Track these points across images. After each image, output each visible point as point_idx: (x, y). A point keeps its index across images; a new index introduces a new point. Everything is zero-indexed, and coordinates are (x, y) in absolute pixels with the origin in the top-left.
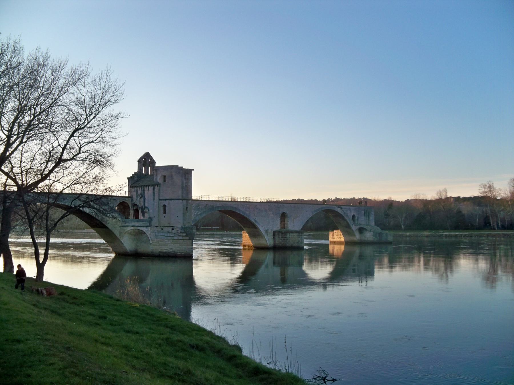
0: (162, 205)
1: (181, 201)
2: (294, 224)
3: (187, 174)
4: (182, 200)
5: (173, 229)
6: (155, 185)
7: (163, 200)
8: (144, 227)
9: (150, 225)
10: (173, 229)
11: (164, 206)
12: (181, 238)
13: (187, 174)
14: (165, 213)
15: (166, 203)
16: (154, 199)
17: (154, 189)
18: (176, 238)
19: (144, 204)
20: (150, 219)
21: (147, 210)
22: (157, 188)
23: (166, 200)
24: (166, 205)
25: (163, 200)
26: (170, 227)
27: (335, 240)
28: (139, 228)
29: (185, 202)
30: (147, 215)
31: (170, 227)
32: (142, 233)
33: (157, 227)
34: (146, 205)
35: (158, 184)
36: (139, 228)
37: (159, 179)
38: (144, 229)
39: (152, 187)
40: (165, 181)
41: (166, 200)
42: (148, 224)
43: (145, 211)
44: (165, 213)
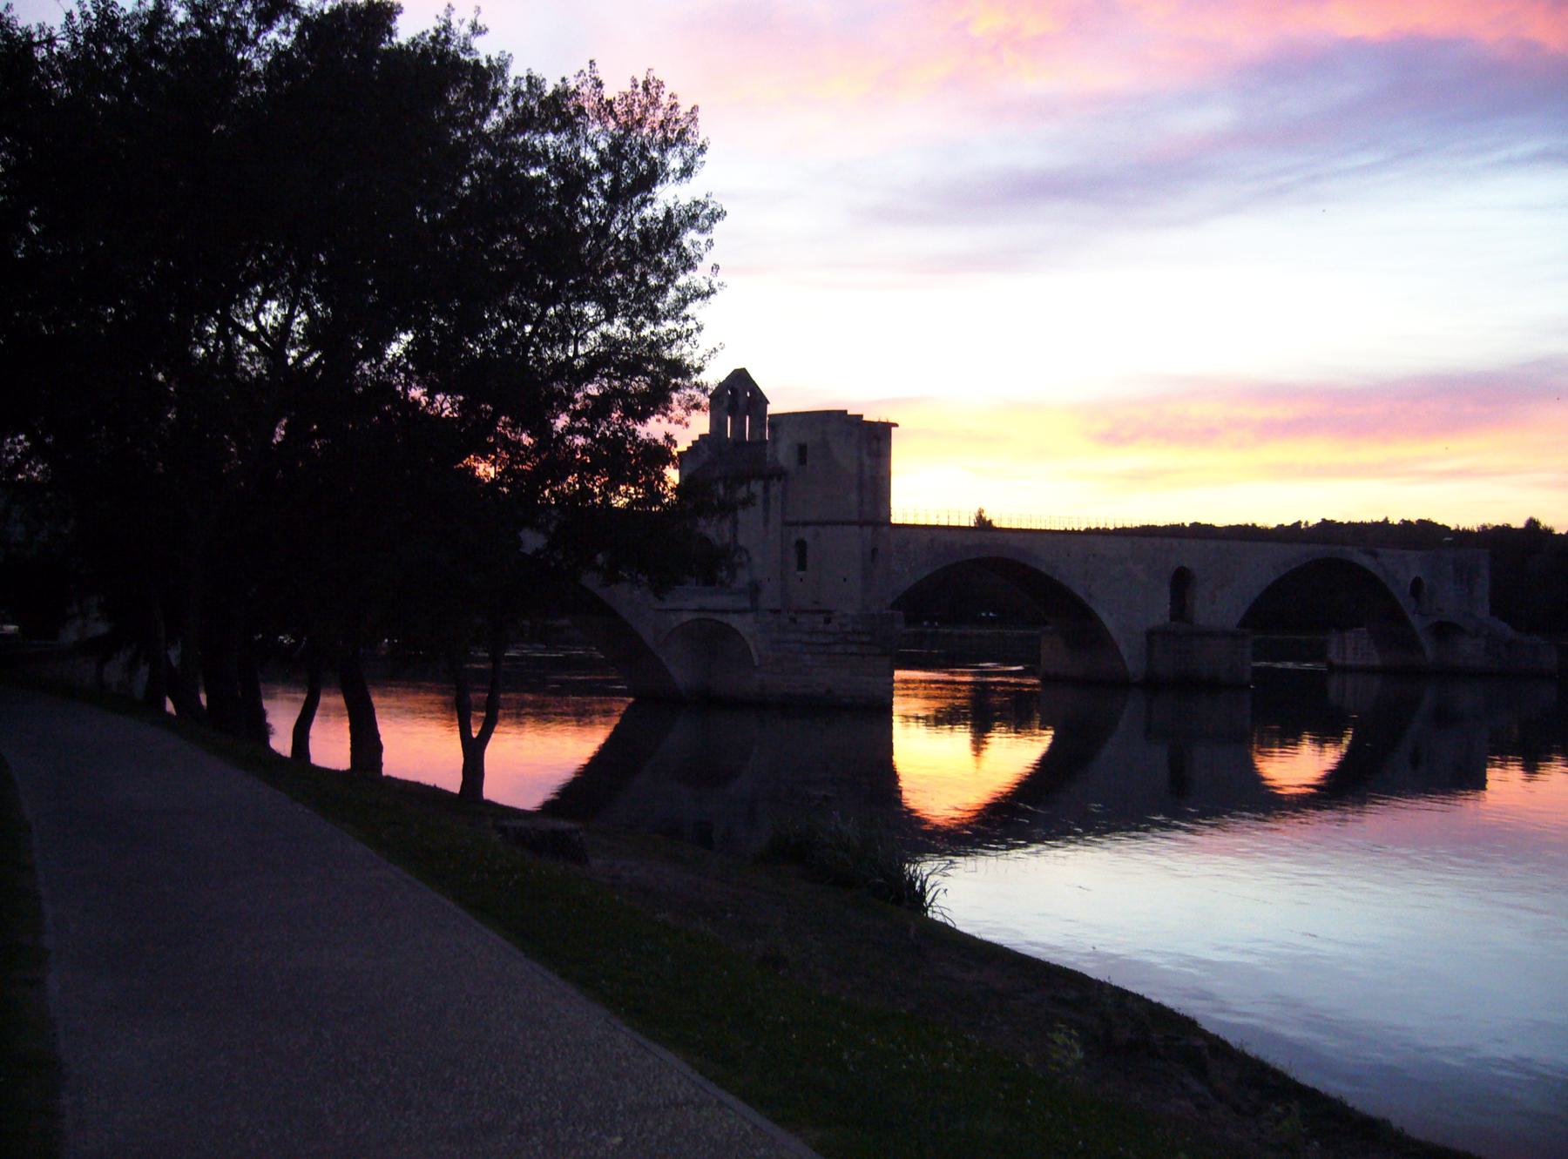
0: (793, 540)
1: (856, 528)
2: (1220, 607)
3: (876, 437)
4: (861, 524)
5: (828, 621)
6: (771, 477)
7: (796, 524)
8: (736, 612)
9: (754, 609)
10: (828, 621)
11: (801, 546)
12: (854, 649)
13: (876, 437)
14: (802, 566)
15: (807, 534)
16: (766, 522)
17: (766, 489)
18: (838, 649)
19: (736, 542)
20: (755, 589)
21: (744, 558)
22: (776, 488)
23: (806, 524)
24: (807, 540)
25: (796, 524)
26: (820, 612)
27: (1348, 662)
28: (717, 617)
29: (868, 530)
30: (743, 577)
31: (820, 612)
32: (730, 632)
33: (776, 611)
34: (741, 542)
35: (780, 474)
36: (717, 617)
37: (784, 455)
38: (735, 621)
39: (761, 483)
40: (802, 460)
41: (806, 524)
42: (748, 605)
43: (736, 559)
44: (802, 566)
